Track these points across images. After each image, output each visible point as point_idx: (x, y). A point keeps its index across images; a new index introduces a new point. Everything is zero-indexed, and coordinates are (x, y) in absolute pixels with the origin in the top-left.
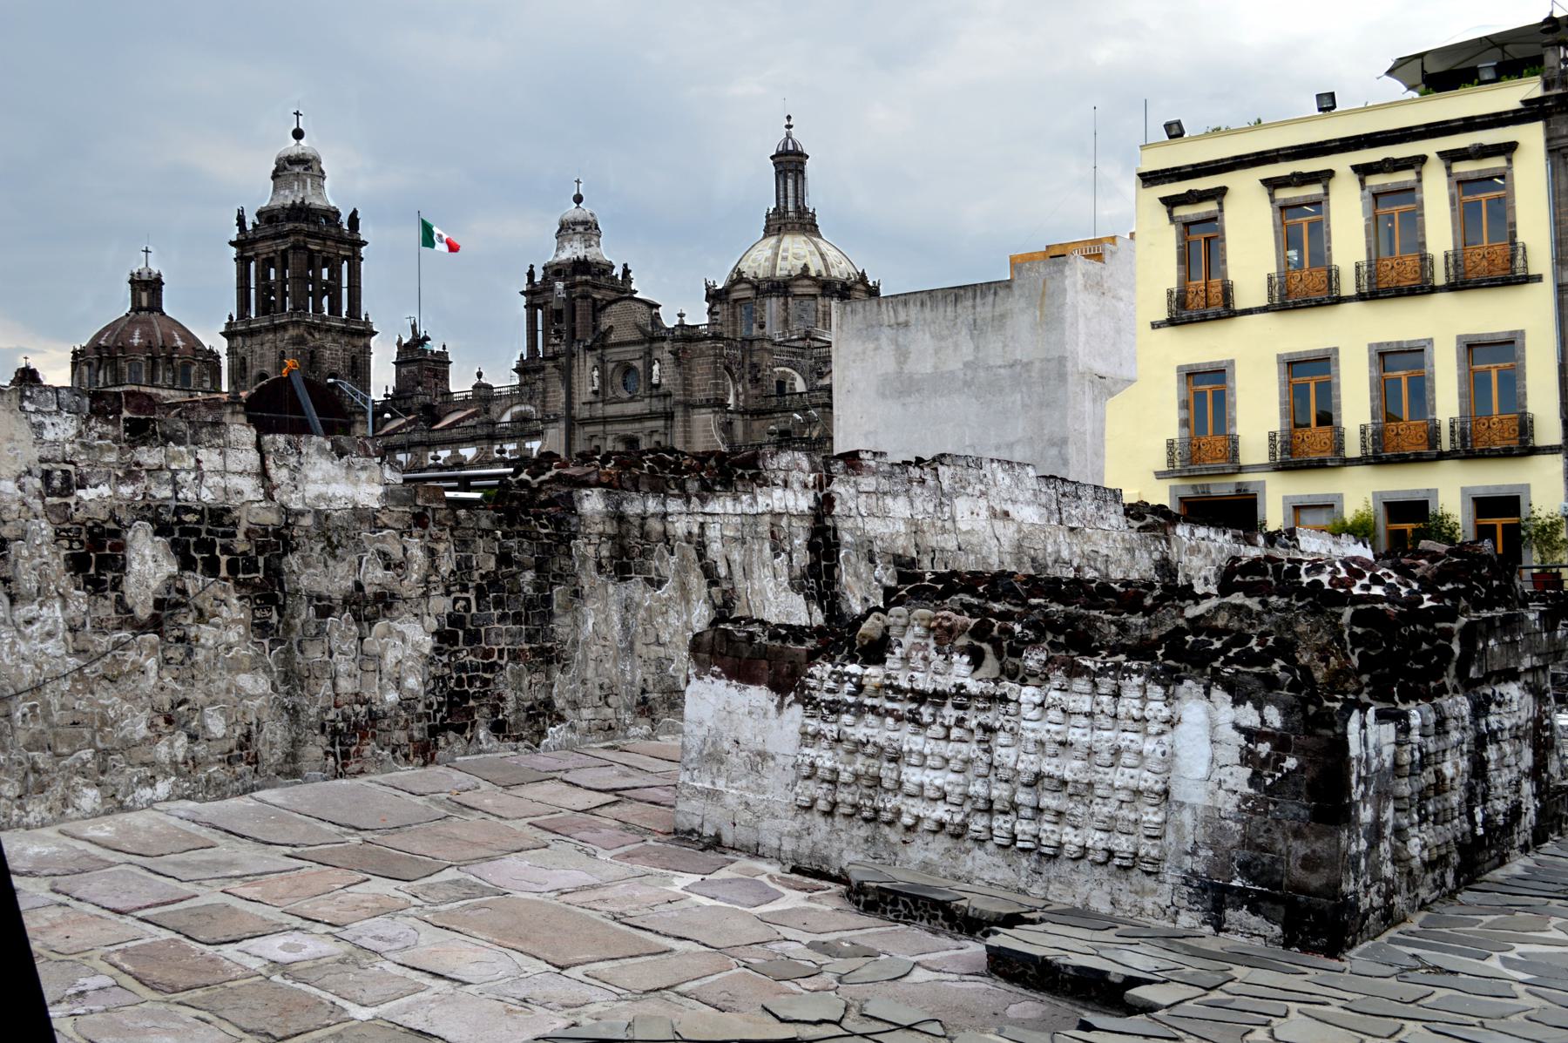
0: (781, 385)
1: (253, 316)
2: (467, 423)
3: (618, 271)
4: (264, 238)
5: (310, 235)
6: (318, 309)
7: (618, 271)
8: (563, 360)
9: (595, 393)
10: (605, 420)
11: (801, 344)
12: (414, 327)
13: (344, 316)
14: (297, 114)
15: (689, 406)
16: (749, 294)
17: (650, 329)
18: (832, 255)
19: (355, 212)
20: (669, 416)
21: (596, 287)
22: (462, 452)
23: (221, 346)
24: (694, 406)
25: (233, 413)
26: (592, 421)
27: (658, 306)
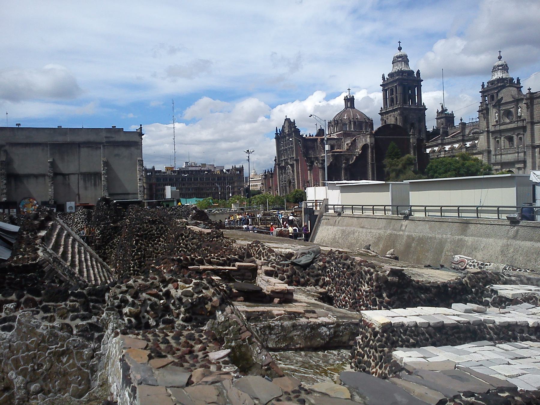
3: (515, 81)
9: (497, 121)
10: (500, 132)
12: (442, 107)
14: (399, 42)
17: (517, 96)
19: (419, 71)
20: (524, 128)
22: (454, 145)
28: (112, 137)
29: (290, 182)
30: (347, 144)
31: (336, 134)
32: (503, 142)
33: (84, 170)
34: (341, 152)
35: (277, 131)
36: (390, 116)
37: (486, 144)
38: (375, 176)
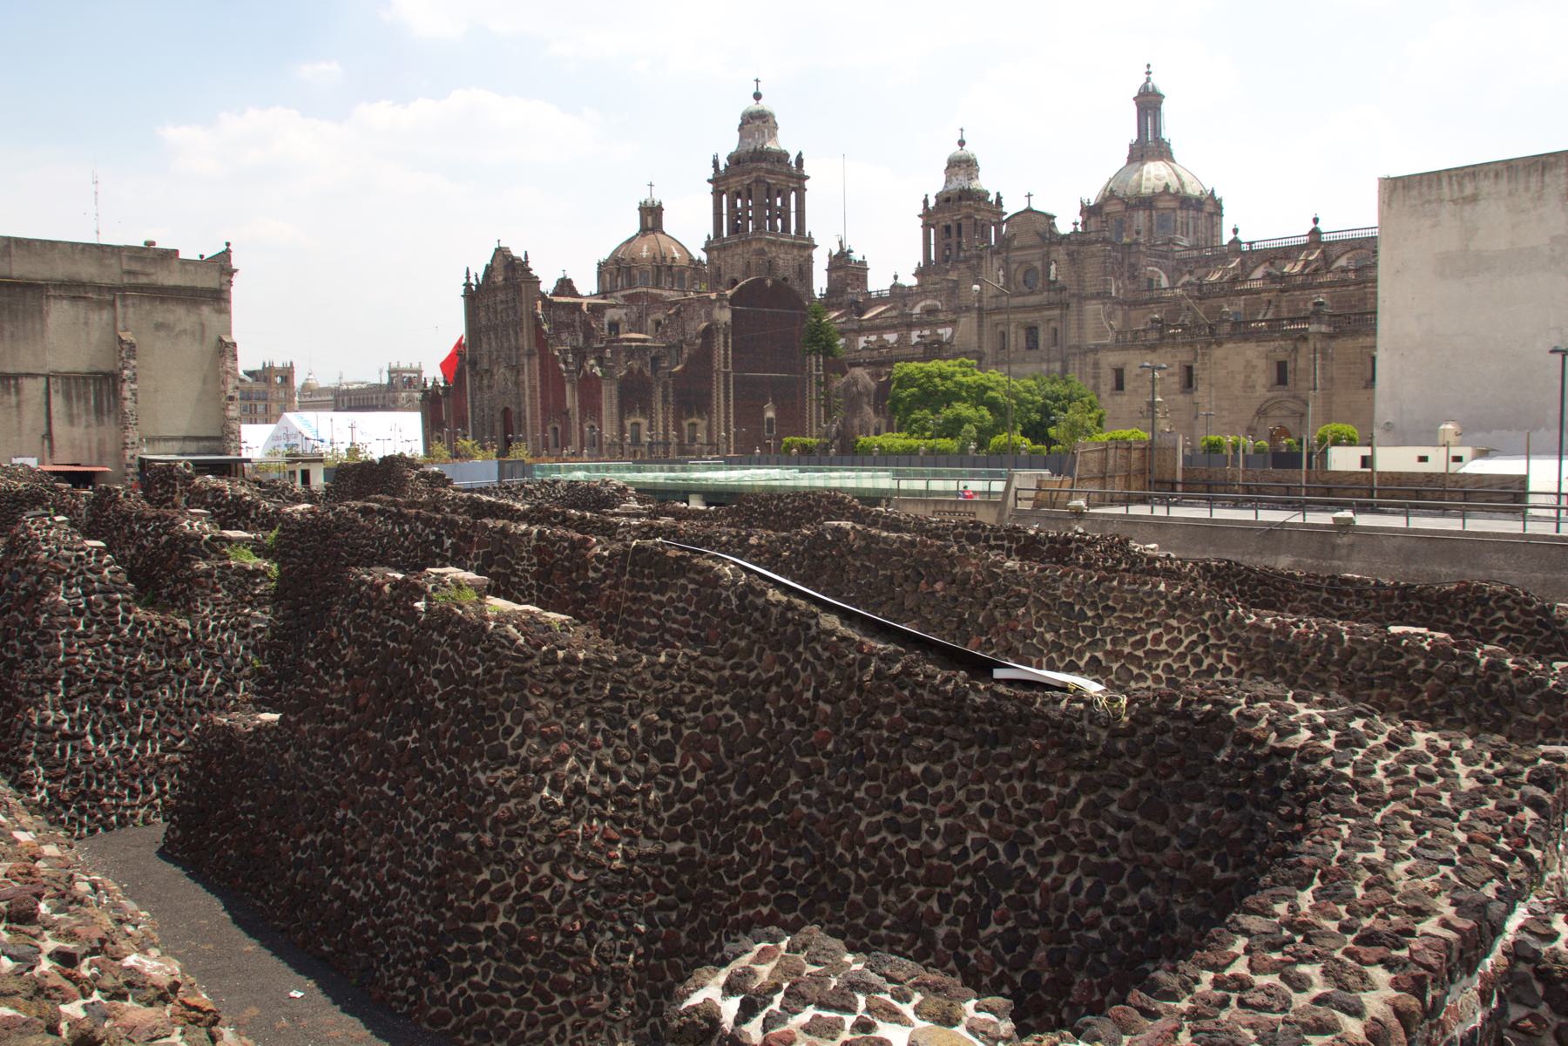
0: (1150, 281)
1: (725, 235)
2: (888, 314)
3: (992, 198)
4: (733, 175)
5: (769, 172)
6: (773, 227)
7: (992, 198)
8: (974, 262)
11: (1165, 248)
12: (841, 242)
13: (793, 233)
14: (757, 81)
15: (1082, 298)
16: (1119, 208)
18: (1186, 178)
19: (800, 154)
21: (977, 210)
22: (886, 337)
23: (704, 257)
24: (1086, 298)
25: (722, 307)
26: (998, 310)
27: (1053, 217)
28: (147, 275)
29: (506, 411)
30: (658, 323)
31: (623, 293)
32: (1017, 338)
33: (66, 366)
34: (644, 341)
35: (468, 278)
36: (733, 256)
37: (975, 338)
38: (732, 402)
